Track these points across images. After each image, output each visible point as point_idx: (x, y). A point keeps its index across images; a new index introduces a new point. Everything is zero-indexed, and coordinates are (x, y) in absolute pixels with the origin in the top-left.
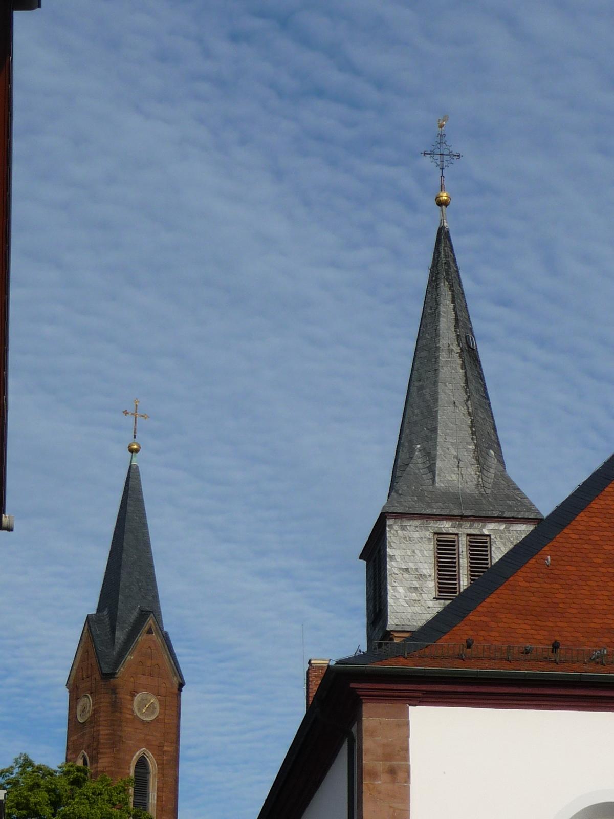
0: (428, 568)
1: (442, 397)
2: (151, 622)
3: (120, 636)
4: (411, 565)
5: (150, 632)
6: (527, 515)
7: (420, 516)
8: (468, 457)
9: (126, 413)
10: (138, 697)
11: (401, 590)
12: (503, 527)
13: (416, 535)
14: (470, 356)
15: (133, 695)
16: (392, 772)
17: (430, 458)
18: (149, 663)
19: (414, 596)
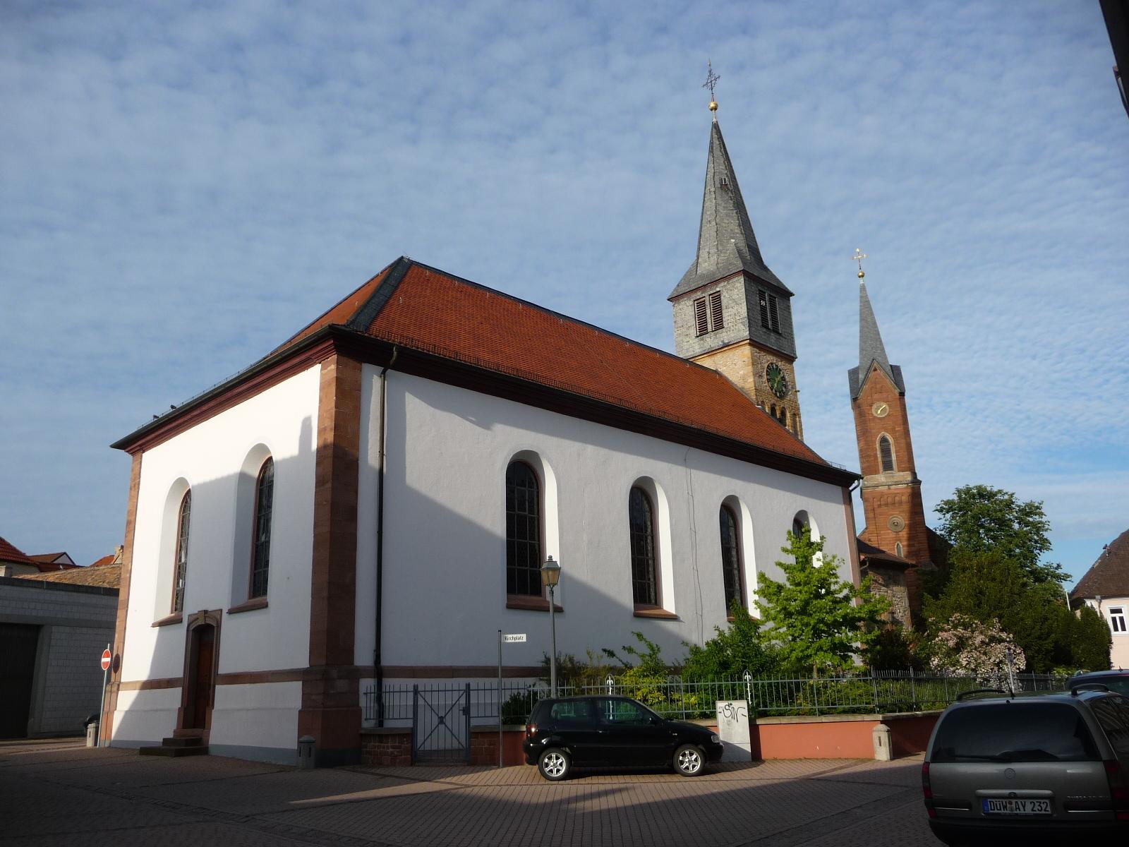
2: (875, 364)
5: (875, 370)
10: (875, 406)
15: (871, 406)
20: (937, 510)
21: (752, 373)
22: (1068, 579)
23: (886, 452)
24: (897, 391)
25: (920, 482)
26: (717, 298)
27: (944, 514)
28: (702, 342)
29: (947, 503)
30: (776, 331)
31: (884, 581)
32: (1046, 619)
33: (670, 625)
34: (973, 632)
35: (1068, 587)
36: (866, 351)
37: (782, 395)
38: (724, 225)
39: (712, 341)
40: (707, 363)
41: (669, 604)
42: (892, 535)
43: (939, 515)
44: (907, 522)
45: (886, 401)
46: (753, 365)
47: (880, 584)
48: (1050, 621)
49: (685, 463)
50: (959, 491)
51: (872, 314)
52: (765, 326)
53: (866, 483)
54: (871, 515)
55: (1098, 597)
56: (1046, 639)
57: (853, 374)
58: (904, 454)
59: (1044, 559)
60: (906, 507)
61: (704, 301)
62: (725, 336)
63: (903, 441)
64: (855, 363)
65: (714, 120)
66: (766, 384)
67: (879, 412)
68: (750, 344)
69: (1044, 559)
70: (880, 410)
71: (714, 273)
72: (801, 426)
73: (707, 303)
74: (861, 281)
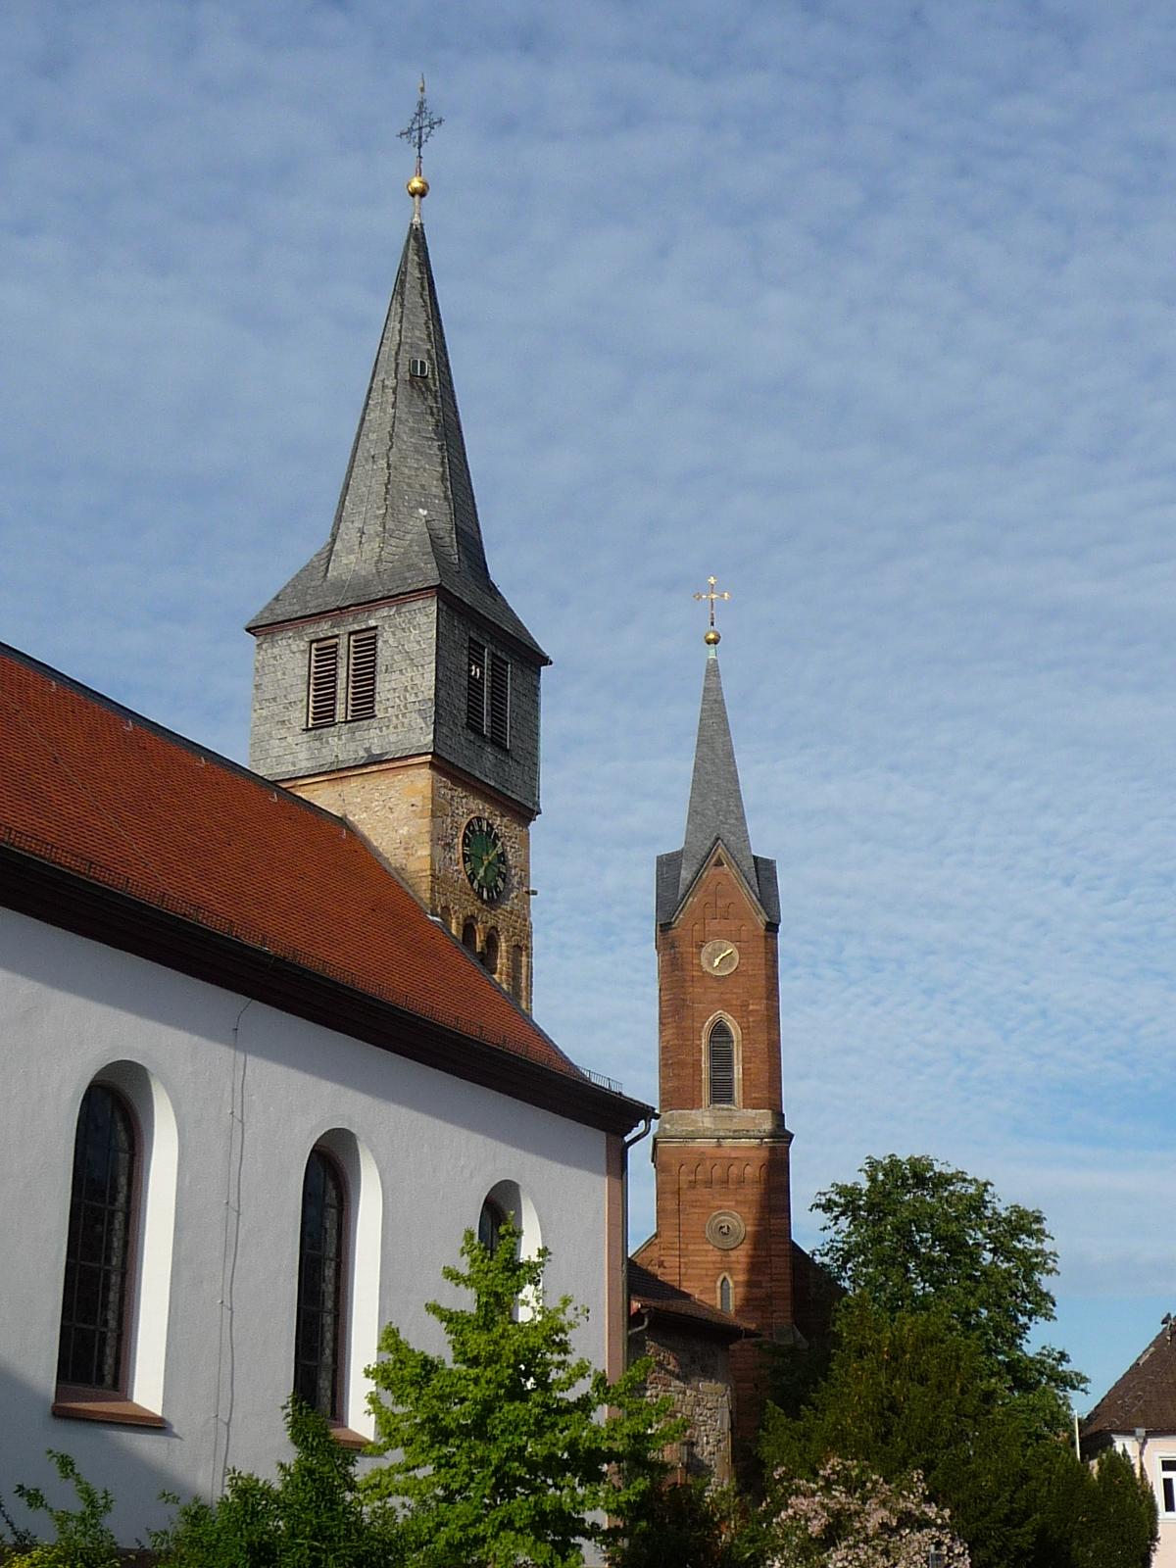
2: (720, 850)
5: (719, 863)
10: (708, 948)
20: (818, 1206)
21: (427, 837)
22: (1082, 1386)
23: (721, 1058)
24: (762, 919)
25: (789, 1137)
26: (367, 644)
27: (836, 1218)
28: (317, 743)
29: (842, 1191)
30: (497, 742)
31: (680, 1365)
32: (1026, 1478)
33: (145, 1444)
34: (864, 1500)
35: (1080, 1405)
36: (704, 815)
37: (493, 903)
38: (406, 471)
39: (340, 745)
40: (323, 796)
41: (147, 1391)
42: (715, 1256)
43: (822, 1218)
44: (749, 1229)
45: (735, 940)
46: (433, 816)
47: (668, 1372)
48: (1033, 1484)
49: (235, 1038)
50: (874, 1165)
51: (727, 732)
52: (474, 726)
53: (668, 1126)
54: (671, 1205)
55: (1141, 1432)
56: (1019, 1525)
57: (668, 865)
58: (760, 1066)
59: (1038, 1339)
60: (752, 1193)
61: (335, 646)
62: (375, 738)
63: (763, 1037)
64: (676, 845)
65: (416, 220)
66: (461, 866)
67: (717, 961)
68: (432, 765)
69: (1038, 1339)
70: (719, 957)
71: (367, 583)
72: (530, 976)
73: (342, 652)
74: (711, 652)
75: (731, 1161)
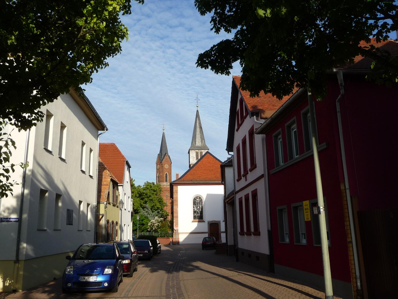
0: (195, 156)
1: (197, 133)
3: (163, 157)
4: (193, 156)
5: (167, 156)
6: (207, 149)
7: (194, 150)
8: (200, 141)
9: (162, 124)
11: (192, 159)
12: (204, 150)
13: (193, 152)
14: (201, 128)
15: (165, 165)
16: (176, 192)
17: (195, 142)
18: (167, 160)
19: (193, 160)
42: (166, 198)
75: (168, 188)
